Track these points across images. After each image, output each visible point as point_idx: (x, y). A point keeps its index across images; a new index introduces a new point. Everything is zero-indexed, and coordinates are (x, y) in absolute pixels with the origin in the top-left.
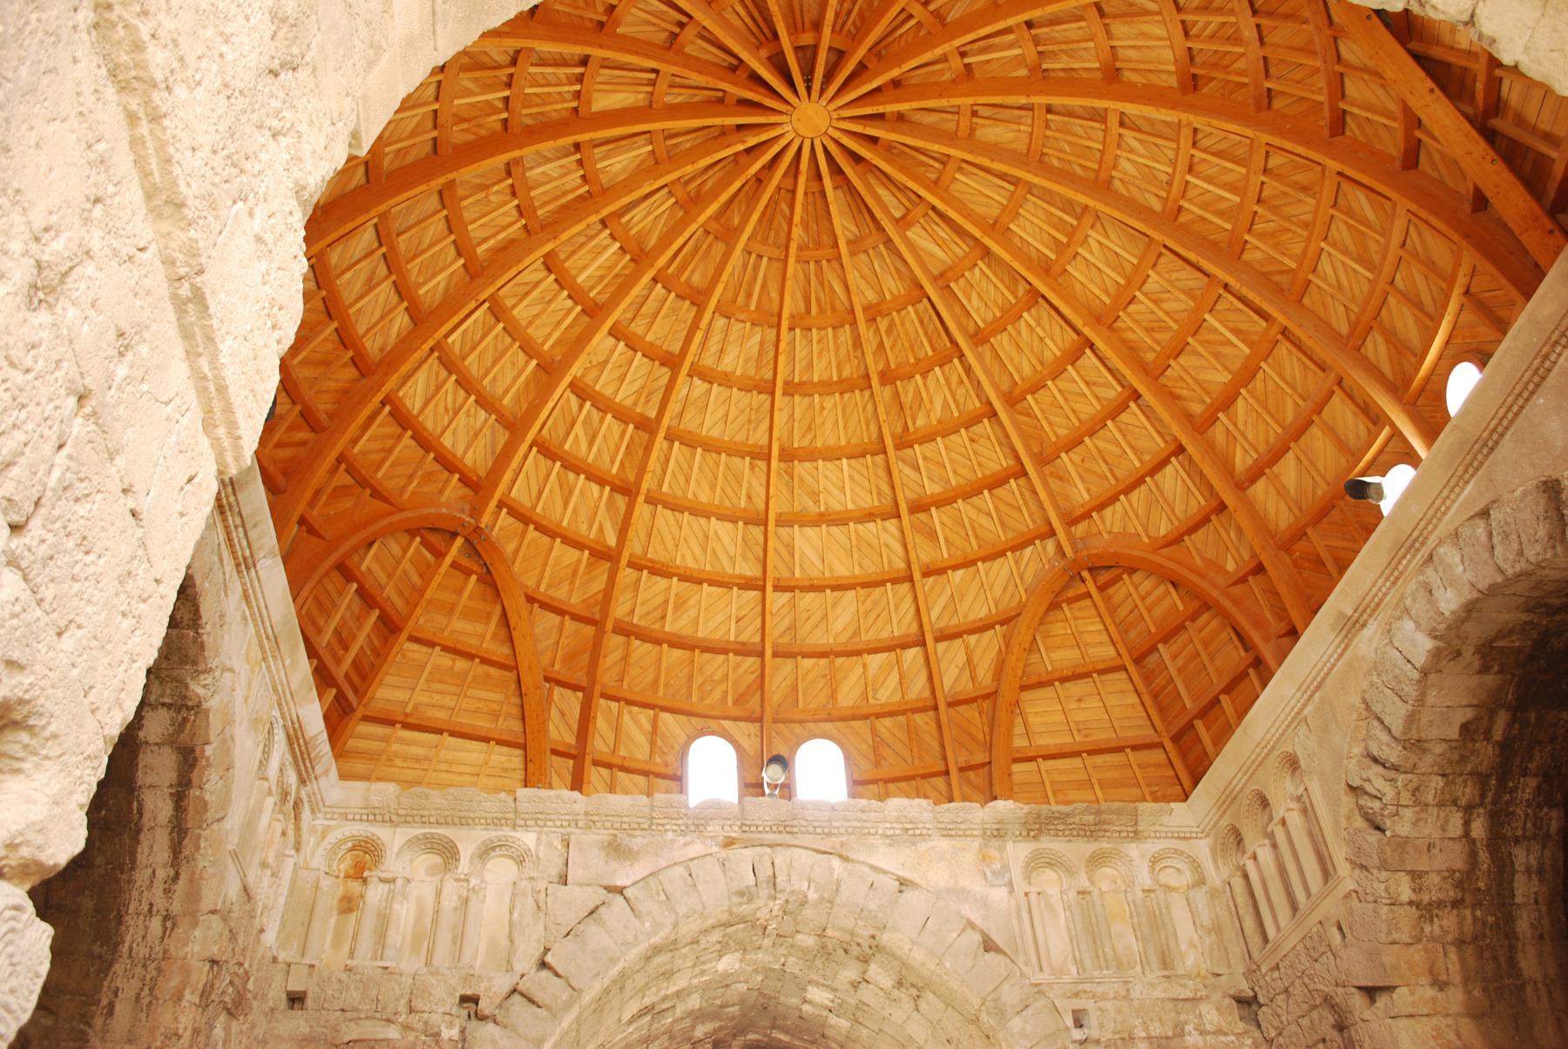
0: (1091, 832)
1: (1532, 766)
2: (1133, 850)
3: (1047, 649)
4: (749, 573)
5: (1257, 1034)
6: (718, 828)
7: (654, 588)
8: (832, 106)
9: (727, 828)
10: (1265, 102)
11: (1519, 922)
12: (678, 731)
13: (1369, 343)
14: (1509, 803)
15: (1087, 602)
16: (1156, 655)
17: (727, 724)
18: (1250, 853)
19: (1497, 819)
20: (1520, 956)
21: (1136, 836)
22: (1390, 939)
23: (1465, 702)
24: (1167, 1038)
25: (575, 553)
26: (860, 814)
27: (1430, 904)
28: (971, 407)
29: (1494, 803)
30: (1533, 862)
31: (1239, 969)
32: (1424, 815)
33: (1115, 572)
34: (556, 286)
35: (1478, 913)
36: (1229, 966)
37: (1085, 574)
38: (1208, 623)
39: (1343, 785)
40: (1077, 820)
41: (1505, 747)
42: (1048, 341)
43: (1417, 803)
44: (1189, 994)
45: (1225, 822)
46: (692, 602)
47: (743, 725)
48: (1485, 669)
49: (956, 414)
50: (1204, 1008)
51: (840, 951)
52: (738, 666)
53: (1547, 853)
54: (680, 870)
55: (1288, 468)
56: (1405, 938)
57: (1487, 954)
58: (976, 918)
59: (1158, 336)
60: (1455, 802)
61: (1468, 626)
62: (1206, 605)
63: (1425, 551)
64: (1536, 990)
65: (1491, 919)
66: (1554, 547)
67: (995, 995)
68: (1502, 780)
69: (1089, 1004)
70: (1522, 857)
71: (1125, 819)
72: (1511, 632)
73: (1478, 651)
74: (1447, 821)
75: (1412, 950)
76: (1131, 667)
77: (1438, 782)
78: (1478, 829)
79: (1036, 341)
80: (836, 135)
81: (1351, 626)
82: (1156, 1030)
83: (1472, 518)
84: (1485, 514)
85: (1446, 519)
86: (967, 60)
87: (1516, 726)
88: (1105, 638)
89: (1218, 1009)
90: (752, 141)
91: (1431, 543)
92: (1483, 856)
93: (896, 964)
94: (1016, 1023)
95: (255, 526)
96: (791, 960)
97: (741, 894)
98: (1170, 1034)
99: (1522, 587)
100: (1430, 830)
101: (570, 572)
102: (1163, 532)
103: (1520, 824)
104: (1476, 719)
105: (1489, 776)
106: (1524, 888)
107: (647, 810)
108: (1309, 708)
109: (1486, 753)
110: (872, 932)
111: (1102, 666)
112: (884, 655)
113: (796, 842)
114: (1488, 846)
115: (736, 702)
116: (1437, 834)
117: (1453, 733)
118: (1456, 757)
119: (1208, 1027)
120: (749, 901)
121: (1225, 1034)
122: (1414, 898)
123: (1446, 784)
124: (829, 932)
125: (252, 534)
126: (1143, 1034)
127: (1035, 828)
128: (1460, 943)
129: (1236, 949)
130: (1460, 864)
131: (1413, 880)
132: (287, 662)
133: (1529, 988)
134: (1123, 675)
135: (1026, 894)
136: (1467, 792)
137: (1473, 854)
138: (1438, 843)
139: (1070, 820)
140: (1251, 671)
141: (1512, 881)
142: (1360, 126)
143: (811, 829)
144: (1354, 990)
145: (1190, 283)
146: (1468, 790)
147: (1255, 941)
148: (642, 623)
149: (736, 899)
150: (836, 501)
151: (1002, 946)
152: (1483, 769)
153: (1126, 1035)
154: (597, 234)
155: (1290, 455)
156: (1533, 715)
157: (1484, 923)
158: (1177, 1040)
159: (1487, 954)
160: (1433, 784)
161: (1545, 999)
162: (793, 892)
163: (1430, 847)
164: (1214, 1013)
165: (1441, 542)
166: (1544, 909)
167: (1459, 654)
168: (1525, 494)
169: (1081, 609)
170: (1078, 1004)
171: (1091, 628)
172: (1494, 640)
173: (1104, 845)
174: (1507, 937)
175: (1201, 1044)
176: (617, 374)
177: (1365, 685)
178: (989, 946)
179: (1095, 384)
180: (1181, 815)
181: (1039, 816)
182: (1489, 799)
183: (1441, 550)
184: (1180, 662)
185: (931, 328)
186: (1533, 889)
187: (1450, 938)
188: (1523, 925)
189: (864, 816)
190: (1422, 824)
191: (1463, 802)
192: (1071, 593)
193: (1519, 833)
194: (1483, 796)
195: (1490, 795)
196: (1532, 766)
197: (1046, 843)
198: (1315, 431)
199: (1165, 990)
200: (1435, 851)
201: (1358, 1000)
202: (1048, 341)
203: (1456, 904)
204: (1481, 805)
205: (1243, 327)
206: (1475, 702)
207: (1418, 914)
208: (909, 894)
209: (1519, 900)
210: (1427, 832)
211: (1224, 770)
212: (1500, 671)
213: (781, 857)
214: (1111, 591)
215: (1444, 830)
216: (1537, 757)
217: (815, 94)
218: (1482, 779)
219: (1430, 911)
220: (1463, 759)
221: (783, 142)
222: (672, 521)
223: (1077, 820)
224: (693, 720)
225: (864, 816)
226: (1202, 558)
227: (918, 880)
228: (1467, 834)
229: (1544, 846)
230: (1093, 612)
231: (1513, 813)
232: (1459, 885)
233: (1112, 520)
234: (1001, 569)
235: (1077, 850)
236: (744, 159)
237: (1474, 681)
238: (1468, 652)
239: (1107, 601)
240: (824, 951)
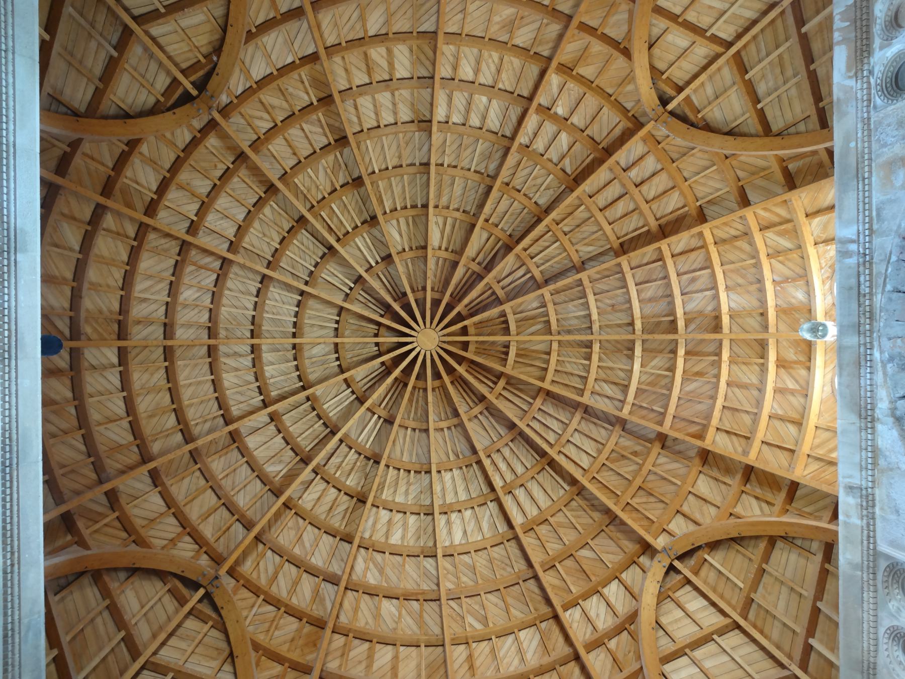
3: (209, 21)
10: (194, 454)
15: (184, 66)
16: (114, 42)
28: (300, 177)
42: (260, 235)
46: (496, 27)
49: (309, 170)
62: (92, 111)
76: (133, 25)
79: (267, 233)
80: (413, 333)
88: (161, 41)
95: (851, 288)
125: (853, 281)
132: (853, 144)
134: (136, 12)
145: (186, 311)
155: (77, 248)
169: (189, 59)
171: (175, 46)
179: (222, 218)
185: (335, 219)
192: (201, 73)
198: (69, 275)
202: (260, 235)
205: (144, 305)
214: (168, 81)
222: (506, 83)
230: (178, 60)
233: (184, 136)
234: (259, 70)
239: (168, 72)
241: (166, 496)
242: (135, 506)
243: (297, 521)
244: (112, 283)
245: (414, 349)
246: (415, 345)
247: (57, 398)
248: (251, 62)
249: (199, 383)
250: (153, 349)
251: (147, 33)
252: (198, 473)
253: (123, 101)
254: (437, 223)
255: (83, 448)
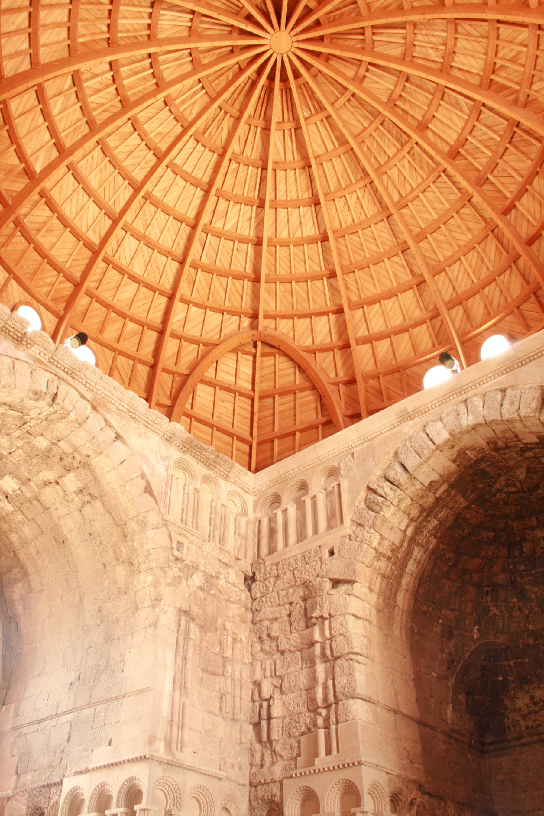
0: (209, 464)
1: (440, 515)
2: (223, 483)
4: (92, 239)
5: (249, 594)
6: (38, 351)
7: (43, 212)
8: (296, 45)
9: (42, 354)
11: (403, 580)
12: (16, 294)
13: (455, 309)
14: (424, 526)
17: (42, 308)
18: (283, 508)
19: (418, 530)
20: (398, 594)
21: (226, 478)
22: (362, 560)
23: (439, 471)
24: (212, 576)
25: (17, 161)
26: (112, 389)
27: (381, 553)
29: (420, 523)
30: (419, 557)
31: (250, 561)
32: (397, 513)
33: (274, 350)
34: (106, 14)
35: (393, 567)
36: (245, 557)
37: (259, 343)
38: (307, 396)
39: (365, 486)
40: (207, 454)
41: (437, 500)
43: (398, 506)
44: (227, 562)
45: (272, 490)
46: (57, 233)
47: (49, 314)
48: (454, 461)
50: (230, 570)
51: (57, 458)
52: (61, 283)
53: (424, 556)
54: (9, 360)
55: (383, 347)
56: (367, 563)
57: (389, 586)
58: (147, 473)
59: (356, 255)
60: (409, 514)
61: (466, 436)
63: (464, 397)
64: (398, 611)
65: (396, 572)
66: (535, 412)
67: (145, 514)
68: (428, 515)
69: (186, 542)
70: (417, 553)
71: (226, 466)
72: (475, 449)
73: (459, 451)
74: (402, 521)
75: (367, 569)
77: (409, 501)
78: (409, 532)
80: (286, 59)
81: (407, 416)
82: (209, 570)
83: (497, 390)
84: (504, 391)
85: (483, 386)
86: (366, 74)
87: (446, 494)
89: (236, 574)
90: (250, 28)
91: (469, 394)
92: (406, 544)
93: (90, 477)
94: (150, 533)
96: (21, 452)
97: (35, 393)
98: (214, 575)
99: (499, 429)
100: (395, 521)
101: (8, 168)
102: (306, 344)
103: (422, 538)
104: (437, 482)
105: (425, 510)
106: (411, 567)
107: (6, 317)
108: (359, 448)
109: (431, 499)
110: (91, 453)
111: (243, 391)
112: (136, 326)
113: (73, 384)
114: (409, 540)
115: (52, 300)
116: (397, 524)
117: (426, 483)
118: (420, 494)
119: (230, 580)
120: (36, 400)
121: (236, 587)
122: (377, 547)
123: (411, 504)
124: (62, 444)
126: (203, 569)
127: (187, 447)
128: (383, 576)
129: (251, 552)
130: (397, 543)
131: (380, 539)
133: (397, 609)
135: (172, 475)
136: (415, 512)
137: (403, 541)
138: (395, 528)
139: (204, 453)
140: (320, 426)
141: (409, 561)
142: (516, 217)
143: (84, 382)
144: (328, 580)
145: (386, 241)
146: (416, 512)
147: (264, 550)
148: (28, 224)
149: (31, 395)
150: (153, 234)
151: (155, 492)
152: (425, 506)
153: (195, 565)
154: (145, 7)
156: (453, 493)
157: (393, 573)
158: (215, 579)
159: (389, 586)
160: (407, 501)
161: (400, 616)
162: (63, 408)
163: (392, 528)
164: (234, 574)
165: (475, 395)
166: (413, 579)
167: (453, 447)
168: (531, 388)
170: (182, 539)
172: (467, 449)
173: (211, 473)
174: (398, 583)
175: (225, 586)
176: (98, 86)
177: (399, 445)
178: (148, 490)
180: (250, 479)
181: (191, 442)
182: (419, 521)
183: (474, 399)
184: (282, 408)
186: (413, 569)
187: (381, 572)
188: (405, 581)
189: (114, 392)
190: (394, 516)
191: (411, 516)
193: (420, 542)
194: (418, 517)
195: (421, 518)
196: (440, 515)
197: (188, 457)
199: (218, 554)
200: (393, 531)
201: (328, 585)
203: (389, 559)
204: (416, 521)
205: (399, 273)
206: (442, 474)
207: (375, 555)
208: (118, 443)
209: (407, 570)
210: (394, 521)
211: (290, 466)
212: (457, 465)
213: (63, 387)
215: (400, 524)
216: (443, 512)
217: (294, 32)
218: (423, 510)
219: (379, 556)
220: (422, 497)
221: (261, 42)
222: (71, 184)
223: (207, 454)
224: (26, 294)
225: (114, 392)
226: (320, 366)
227: (126, 439)
228: (405, 531)
229: (425, 553)
231: (422, 532)
232: (393, 551)
235: (200, 469)
236: (235, 34)
237: (449, 463)
238: (457, 448)
240: (47, 454)
241: (519, 196)
242: (535, 218)
243: (499, 68)
244: (396, 305)
245: (299, 48)
246: (293, 50)
247: (482, 304)
248: (215, 328)
249: (429, 202)
250: (423, 251)
251: (253, 390)
252: (495, 172)
253: (295, 373)
254: (191, 113)
255: (508, 272)
